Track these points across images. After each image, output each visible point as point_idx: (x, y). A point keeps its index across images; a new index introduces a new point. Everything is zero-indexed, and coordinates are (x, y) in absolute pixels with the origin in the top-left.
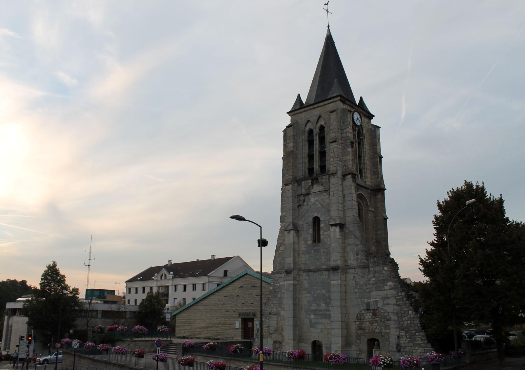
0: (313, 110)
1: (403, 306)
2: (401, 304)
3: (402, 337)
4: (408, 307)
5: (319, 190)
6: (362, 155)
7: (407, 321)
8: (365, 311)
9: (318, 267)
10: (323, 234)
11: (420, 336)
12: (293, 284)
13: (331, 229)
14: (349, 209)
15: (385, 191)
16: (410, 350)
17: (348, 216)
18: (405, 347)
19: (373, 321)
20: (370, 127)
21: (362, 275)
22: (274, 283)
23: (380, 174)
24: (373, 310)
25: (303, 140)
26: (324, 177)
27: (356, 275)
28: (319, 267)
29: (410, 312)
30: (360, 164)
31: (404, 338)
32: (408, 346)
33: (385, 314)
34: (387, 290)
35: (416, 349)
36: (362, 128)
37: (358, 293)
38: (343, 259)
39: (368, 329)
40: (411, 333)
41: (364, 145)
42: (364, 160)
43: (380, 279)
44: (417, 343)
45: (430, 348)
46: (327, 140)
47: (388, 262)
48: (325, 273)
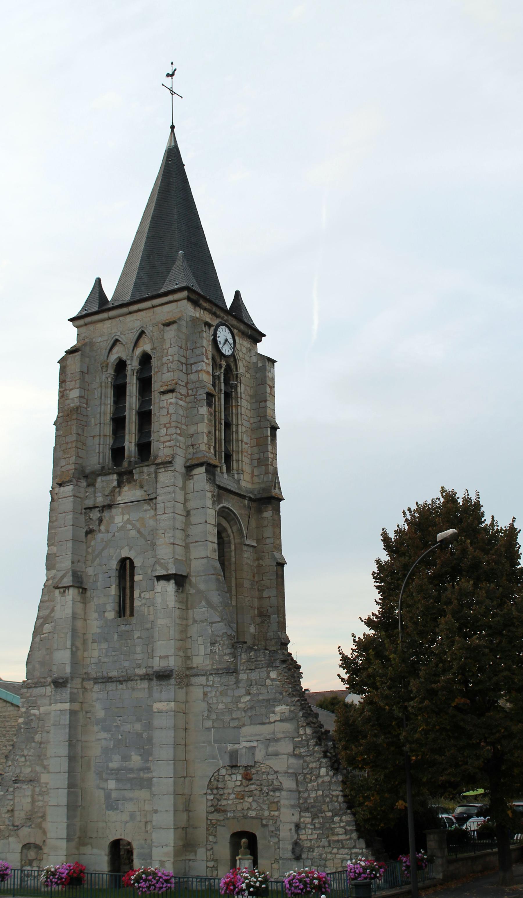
0: (128, 316)
1: (308, 759)
2: (303, 754)
3: (305, 826)
4: (318, 760)
5: (133, 499)
6: (234, 423)
7: (316, 790)
8: (226, 769)
9: (126, 671)
10: (140, 596)
11: (343, 824)
12: (70, 710)
13: (156, 587)
14: (198, 542)
15: (282, 503)
16: (321, 855)
17: (195, 559)
18: (311, 848)
19: (243, 791)
20: (254, 359)
21: (221, 689)
22: (27, 709)
23: (272, 465)
24: (244, 769)
25: (103, 384)
26: (145, 469)
27: (208, 689)
28: (128, 671)
29: (323, 771)
30: (228, 440)
31: (309, 828)
32: (318, 847)
33: (270, 777)
34: (275, 722)
35: (333, 851)
36: (235, 360)
37: (212, 729)
38: (181, 654)
39: (234, 811)
40: (323, 817)
41: (239, 400)
42: (237, 432)
43: (261, 698)
44: (336, 838)
45: (362, 849)
46: (156, 386)
47: (278, 661)
48: (142, 686)
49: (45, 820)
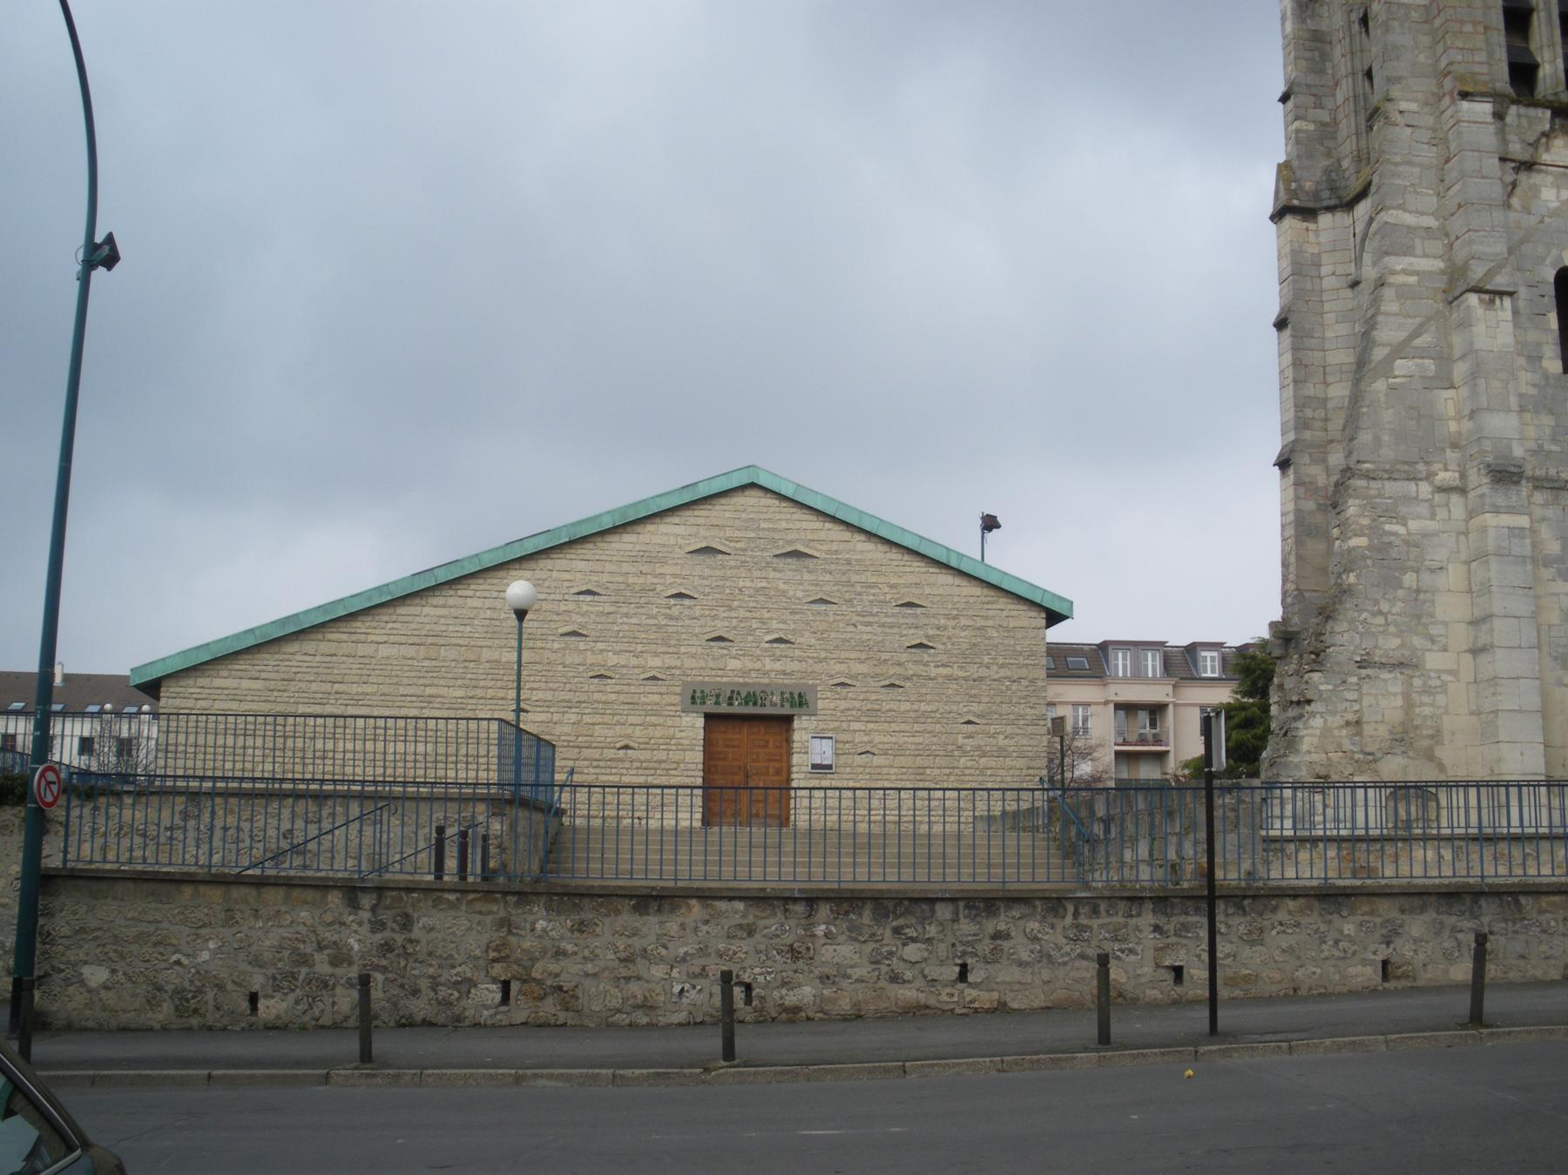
22: (1374, 520)
49: (1440, 743)
